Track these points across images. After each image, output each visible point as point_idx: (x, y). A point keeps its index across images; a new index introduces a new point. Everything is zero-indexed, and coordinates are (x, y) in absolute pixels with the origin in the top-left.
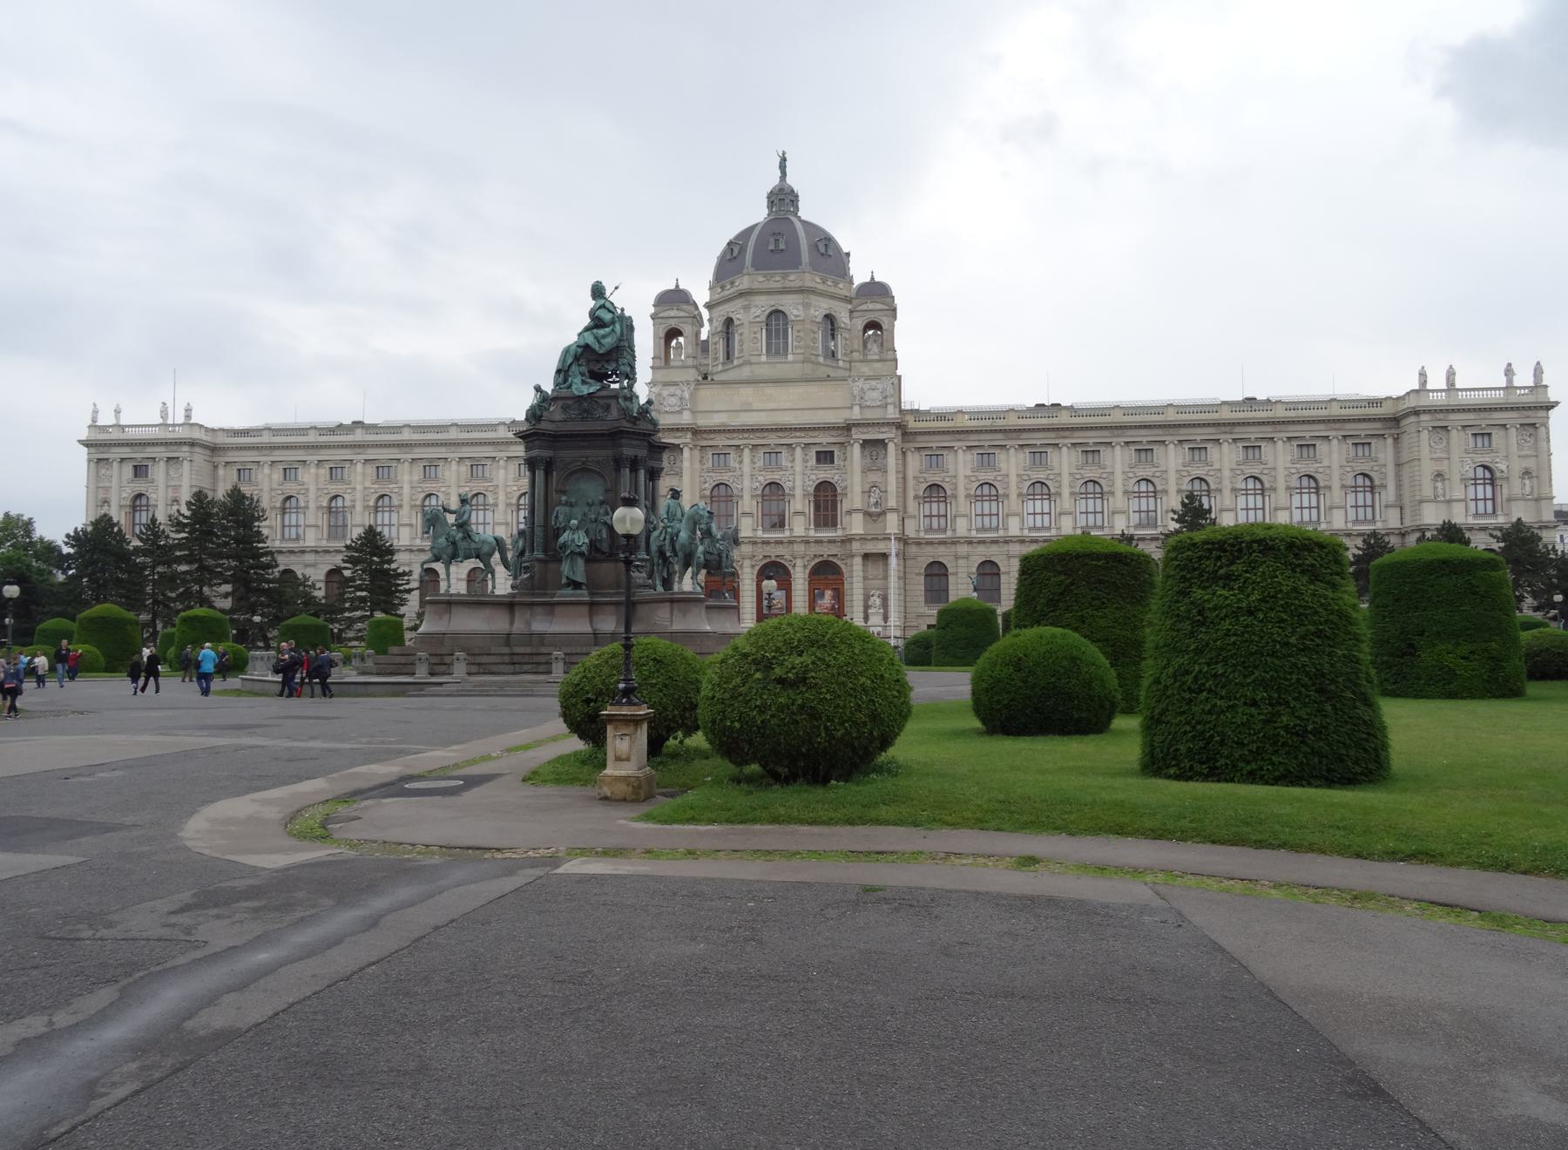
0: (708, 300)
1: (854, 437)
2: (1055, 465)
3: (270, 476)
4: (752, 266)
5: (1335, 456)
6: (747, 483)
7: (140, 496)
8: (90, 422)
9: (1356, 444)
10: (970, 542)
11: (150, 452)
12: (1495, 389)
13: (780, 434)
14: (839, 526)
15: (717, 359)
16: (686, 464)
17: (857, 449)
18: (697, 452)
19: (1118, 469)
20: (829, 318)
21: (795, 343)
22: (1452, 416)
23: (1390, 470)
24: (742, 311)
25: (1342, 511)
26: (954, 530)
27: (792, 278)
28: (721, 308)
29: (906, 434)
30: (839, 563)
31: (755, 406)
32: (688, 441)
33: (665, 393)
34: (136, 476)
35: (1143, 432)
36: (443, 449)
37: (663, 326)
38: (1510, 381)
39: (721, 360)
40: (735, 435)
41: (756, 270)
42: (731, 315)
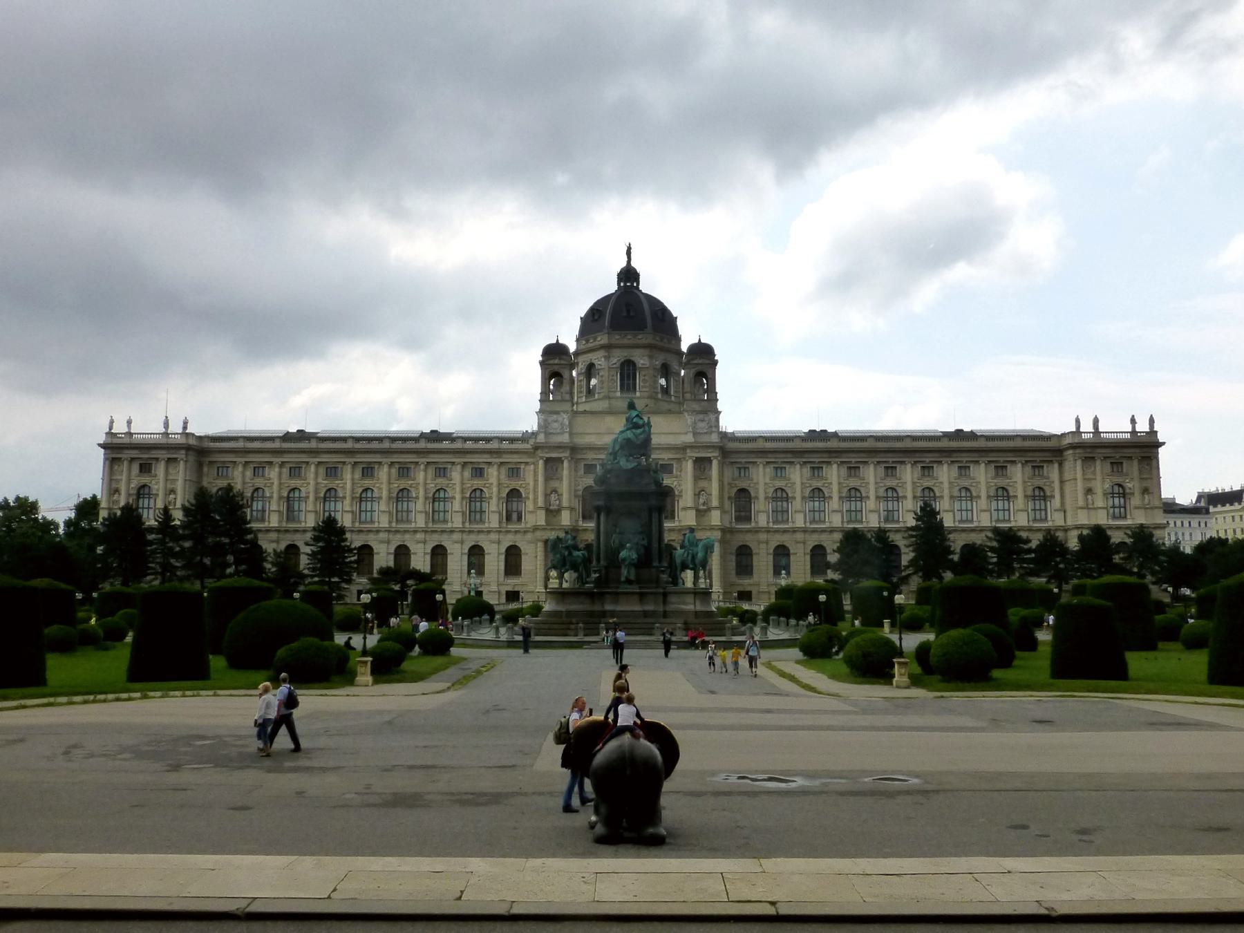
1: (688, 455)
2: (829, 476)
3: (244, 476)
8: (107, 430)
10: (768, 531)
12: (1125, 432)
14: (676, 519)
16: (565, 472)
19: (872, 480)
21: (641, 384)
23: (1057, 485)
24: (603, 359)
26: (757, 522)
27: (640, 337)
28: (585, 356)
29: (725, 453)
36: (378, 456)
37: (548, 370)
38: (1134, 427)
41: (613, 330)
42: (594, 361)
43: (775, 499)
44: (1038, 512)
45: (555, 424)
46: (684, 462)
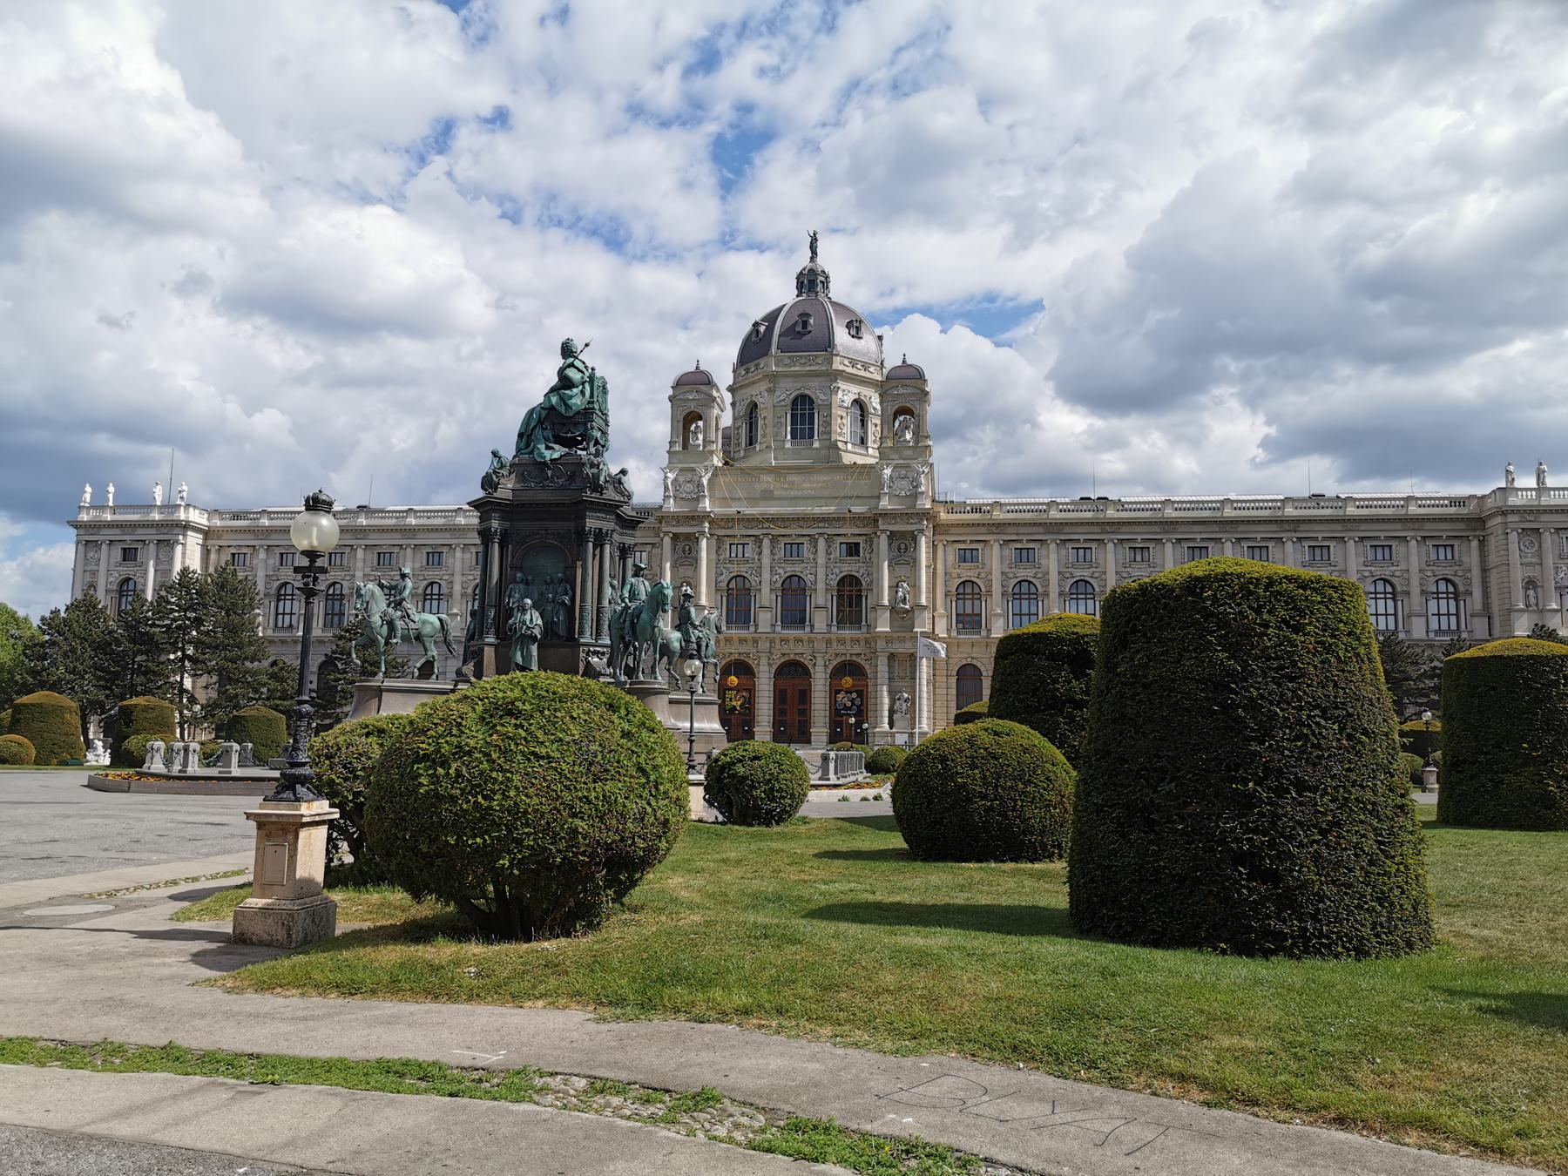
0: (731, 383)
1: (881, 528)
2: (1101, 562)
5: (1414, 559)
6: (766, 575)
7: (128, 580)
9: (1438, 546)
11: (141, 534)
15: (738, 445)
17: (883, 541)
18: (714, 542)
20: (859, 404)
22: (1544, 518)
23: (1476, 574)
25: (1424, 619)
28: (743, 391)
30: (863, 663)
33: (681, 479)
34: (124, 560)
35: (1196, 528)
39: (744, 445)
42: (759, 400)
43: (1017, 596)
44: (1444, 619)
45: (689, 485)
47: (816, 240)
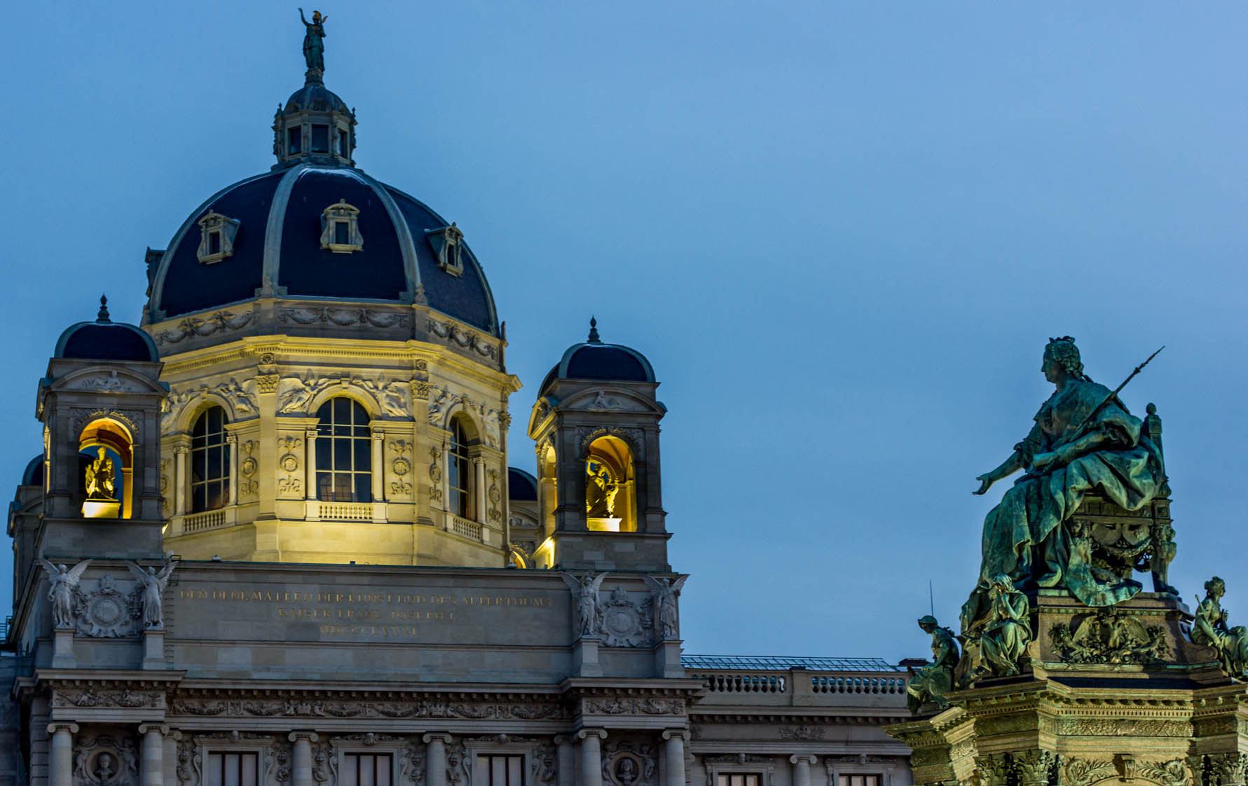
1: (587, 720)
4: (281, 283)
13: (388, 707)
31: (327, 632)
32: (160, 715)
40: (274, 705)
41: (290, 292)
45: (108, 604)
46: (564, 751)
47: (321, 34)
